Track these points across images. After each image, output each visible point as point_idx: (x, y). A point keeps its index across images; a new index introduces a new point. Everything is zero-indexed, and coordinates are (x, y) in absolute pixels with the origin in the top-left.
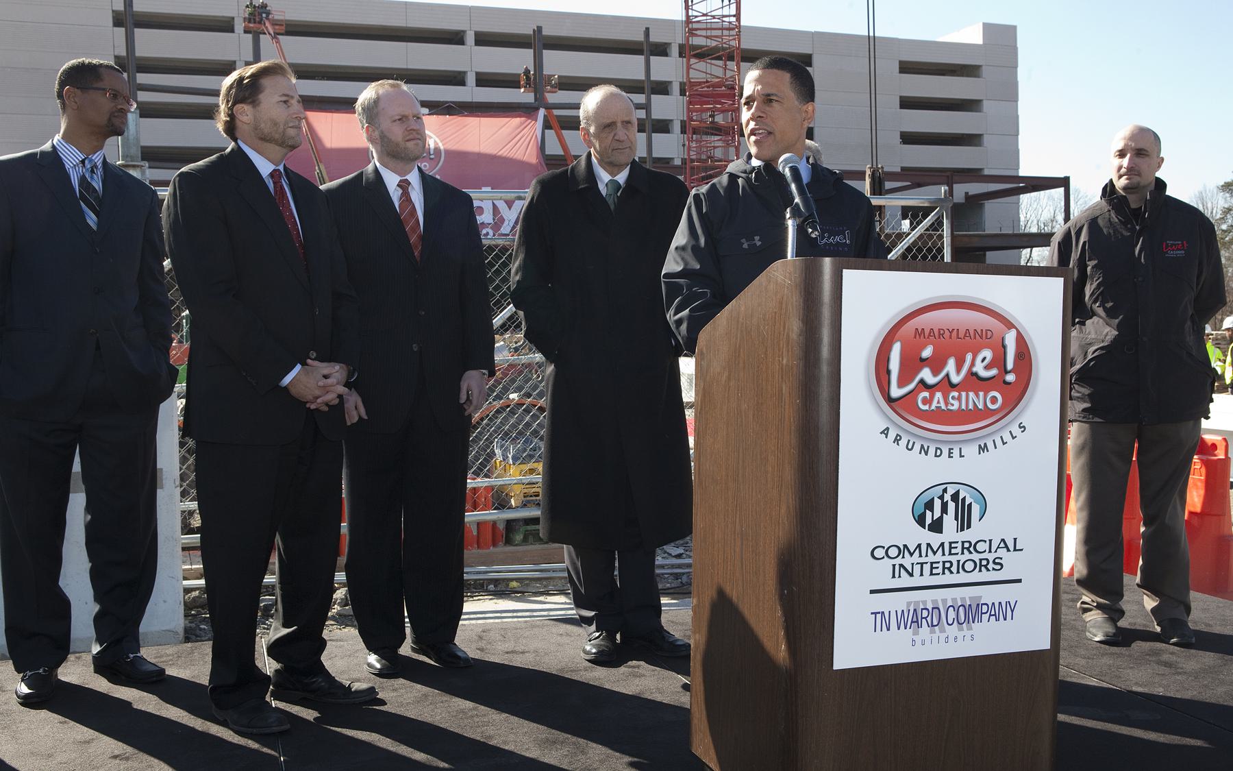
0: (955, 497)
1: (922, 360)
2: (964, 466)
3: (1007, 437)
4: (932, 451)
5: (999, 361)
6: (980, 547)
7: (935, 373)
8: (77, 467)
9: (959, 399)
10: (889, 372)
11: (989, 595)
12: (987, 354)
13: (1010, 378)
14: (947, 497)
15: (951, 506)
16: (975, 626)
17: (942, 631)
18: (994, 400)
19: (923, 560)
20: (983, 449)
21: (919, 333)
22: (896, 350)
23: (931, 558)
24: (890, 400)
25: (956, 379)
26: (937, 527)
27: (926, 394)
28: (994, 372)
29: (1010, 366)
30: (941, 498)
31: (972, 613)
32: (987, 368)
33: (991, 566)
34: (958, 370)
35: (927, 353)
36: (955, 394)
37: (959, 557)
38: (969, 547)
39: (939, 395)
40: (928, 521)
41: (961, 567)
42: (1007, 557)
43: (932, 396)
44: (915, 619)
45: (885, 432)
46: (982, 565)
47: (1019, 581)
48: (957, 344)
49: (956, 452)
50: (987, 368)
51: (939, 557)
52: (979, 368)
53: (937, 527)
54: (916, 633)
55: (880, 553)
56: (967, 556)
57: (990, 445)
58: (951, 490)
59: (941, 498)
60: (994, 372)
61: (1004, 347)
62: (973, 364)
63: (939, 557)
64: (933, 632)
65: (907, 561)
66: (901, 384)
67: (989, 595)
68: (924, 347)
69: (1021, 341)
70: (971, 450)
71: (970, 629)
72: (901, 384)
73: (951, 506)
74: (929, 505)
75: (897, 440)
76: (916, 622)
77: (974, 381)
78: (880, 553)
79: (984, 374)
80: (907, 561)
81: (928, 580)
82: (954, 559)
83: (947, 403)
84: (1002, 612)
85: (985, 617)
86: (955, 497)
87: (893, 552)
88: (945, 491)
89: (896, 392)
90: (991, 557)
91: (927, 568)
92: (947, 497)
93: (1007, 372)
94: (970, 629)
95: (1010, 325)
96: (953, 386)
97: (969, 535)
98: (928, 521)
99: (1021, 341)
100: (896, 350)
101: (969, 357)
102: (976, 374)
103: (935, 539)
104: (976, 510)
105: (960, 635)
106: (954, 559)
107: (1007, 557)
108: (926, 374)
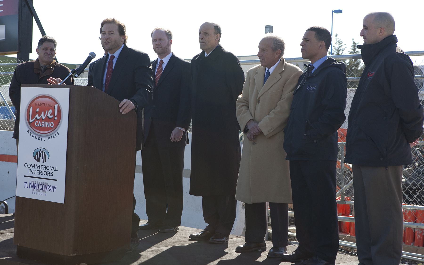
0: (42, 152)
1: (37, 112)
2: (45, 144)
3: (55, 136)
4: (38, 138)
5: (53, 114)
6: (48, 168)
7: (39, 116)
8: (139, 162)
9: (44, 124)
10: (29, 115)
11: (50, 183)
12: (51, 111)
13: (56, 118)
14: (41, 152)
15: (42, 154)
16: (46, 191)
17: (39, 191)
18: (52, 124)
19: (35, 169)
20: (49, 139)
21: (36, 104)
22: (31, 108)
23: (37, 169)
24: (29, 123)
25: (44, 118)
26: (38, 160)
27: (37, 122)
28: (52, 116)
29: (56, 115)
30: (39, 152)
31: (46, 187)
32: (51, 115)
33: (50, 174)
34: (44, 116)
35: (38, 110)
36: (43, 122)
37: (43, 170)
38: (45, 167)
39: (40, 122)
40: (37, 158)
41: (44, 173)
42: (54, 172)
43: (38, 122)
44: (33, 186)
45: (28, 132)
46: (48, 174)
47: (57, 180)
48: (44, 108)
49: (43, 139)
50: (51, 115)
51: (38, 169)
52: (49, 115)
53: (38, 160)
54: (33, 190)
55: (26, 165)
56: (45, 170)
57: (51, 138)
58: (42, 150)
59: (39, 152)
60: (52, 116)
61: (55, 109)
62: (47, 114)
63: (38, 169)
64: (37, 191)
65: (32, 169)
66: (32, 119)
67: (50, 183)
68: (37, 109)
69: (59, 107)
70: (46, 139)
71: (45, 192)
72: (32, 119)
73: (42, 154)
74: (37, 154)
75: (30, 134)
76: (33, 187)
77: (48, 119)
78: (26, 165)
79: (50, 117)
80: (32, 169)
81: (36, 175)
82: (42, 170)
83: (41, 125)
84: (53, 189)
85: (49, 189)
86: (42, 152)
87: (29, 166)
88: (40, 150)
89: (31, 121)
90: (50, 171)
91: (36, 171)
92: (41, 152)
93: (55, 117)
94: (45, 192)
95: (56, 103)
96: (43, 120)
97: (46, 164)
98: (37, 158)
99: (59, 107)
100: (31, 108)
101: (47, 112)
102: (48, 117)
103: (38, 164)
104: (47, 156)
105: (43, 193)
106: (42, 170)
107: (54, 172)
108: (37, 116)
